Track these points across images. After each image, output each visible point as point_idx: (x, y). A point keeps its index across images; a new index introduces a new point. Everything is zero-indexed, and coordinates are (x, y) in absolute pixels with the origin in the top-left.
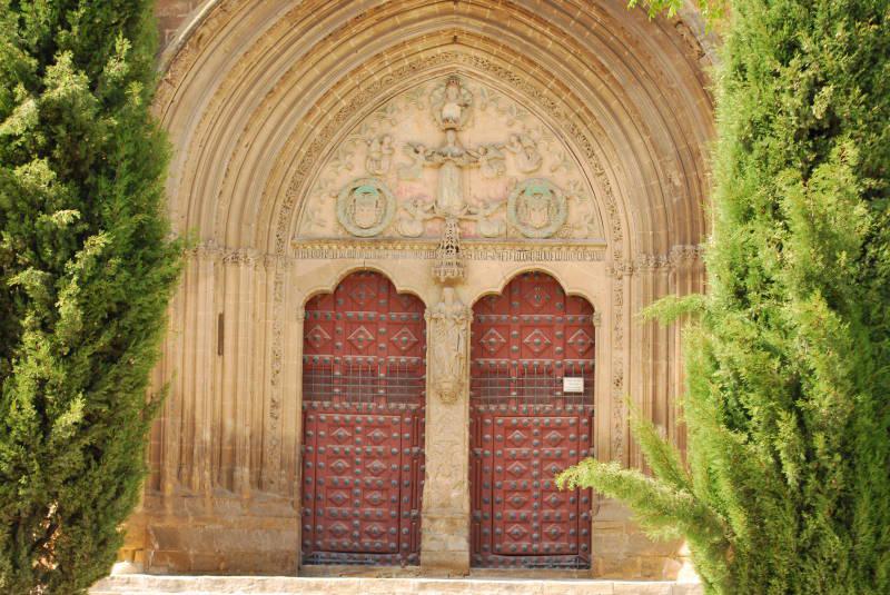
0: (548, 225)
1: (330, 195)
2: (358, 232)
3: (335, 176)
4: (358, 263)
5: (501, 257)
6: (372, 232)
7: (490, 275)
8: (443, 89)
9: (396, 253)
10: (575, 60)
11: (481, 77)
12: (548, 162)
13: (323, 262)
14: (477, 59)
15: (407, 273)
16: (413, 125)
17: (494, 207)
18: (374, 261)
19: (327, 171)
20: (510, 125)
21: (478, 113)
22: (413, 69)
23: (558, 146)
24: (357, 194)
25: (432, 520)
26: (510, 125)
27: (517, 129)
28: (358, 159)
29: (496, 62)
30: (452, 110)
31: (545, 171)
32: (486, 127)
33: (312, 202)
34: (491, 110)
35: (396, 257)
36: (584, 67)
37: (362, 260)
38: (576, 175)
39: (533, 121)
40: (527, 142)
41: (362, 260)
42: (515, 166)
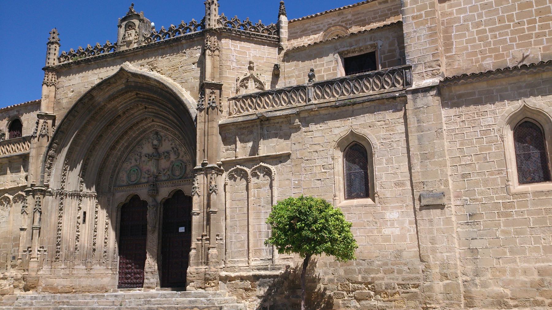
0: (181, 174)
2: (131, 183)
3: (127, 166)
4: (131, 192)
6: (135, 182)
7: (165, 192)
12: (182, 154)
13: (122, 193)
15: (143, 193)
16: (147, 149)
17: (166, 170)
19: (125, 165)
20: (172, 144)
21: (163, 142)
22: (144, 131)
24: (132, 171)
25: (147, 273)
26: (172, 144)
27: (173, 146)
28: (133, 161)
30: (155, 142)
31: (180, 158)
32: (166, 146)
33: (121, 175)
34: (167, 141)
40: (175, 149)
42: (173, 157)
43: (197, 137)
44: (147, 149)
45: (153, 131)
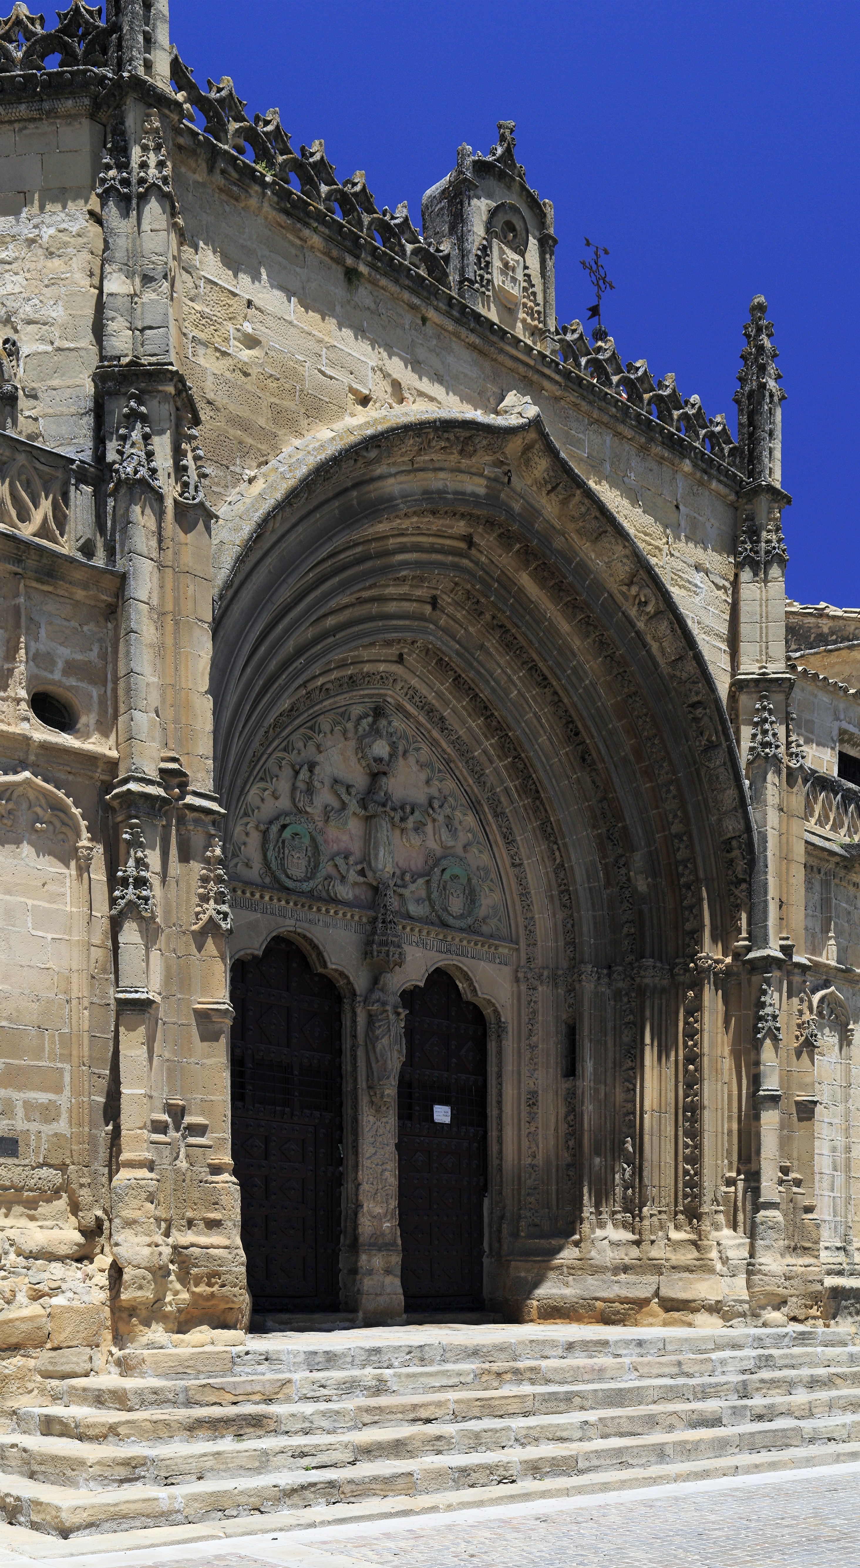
1: (257, 827)
5: (425, 945)
8: (370, 719)
9: (328, 920)
10: (534, 720)
11: (408, 715)
14: (416, 691)
18: (306, 925)
23: (470, 820)
29: (434, 701)
34: (411, 760)
35: (327, 925)
36: (542, 732)
37: (293, 922)
38: (485, 859)
39: (450, 785)
41: (293, 922)
43: (769, 854)
44: (339, 760)
45: (370, 696)
